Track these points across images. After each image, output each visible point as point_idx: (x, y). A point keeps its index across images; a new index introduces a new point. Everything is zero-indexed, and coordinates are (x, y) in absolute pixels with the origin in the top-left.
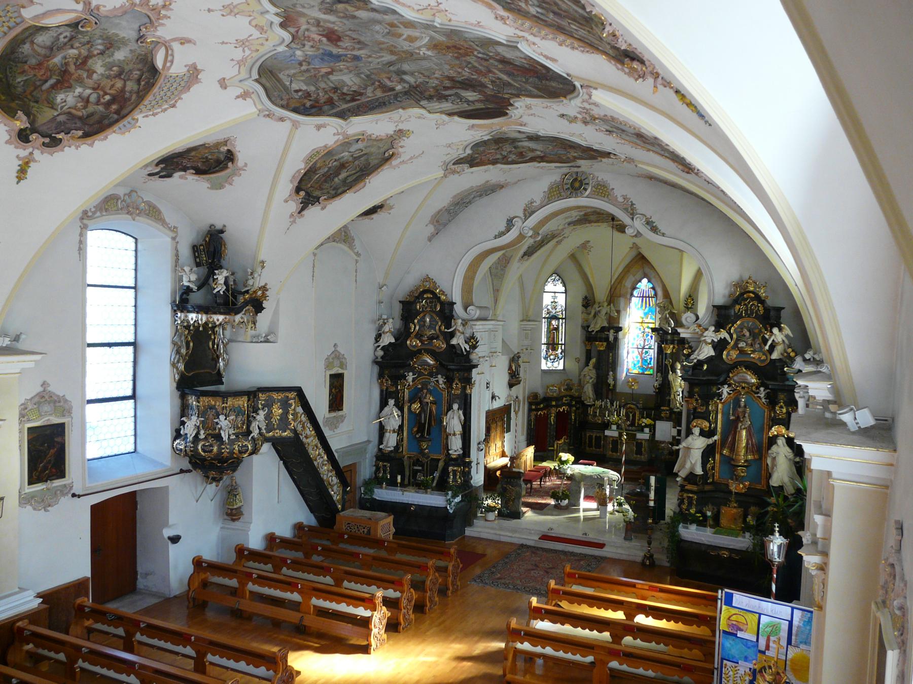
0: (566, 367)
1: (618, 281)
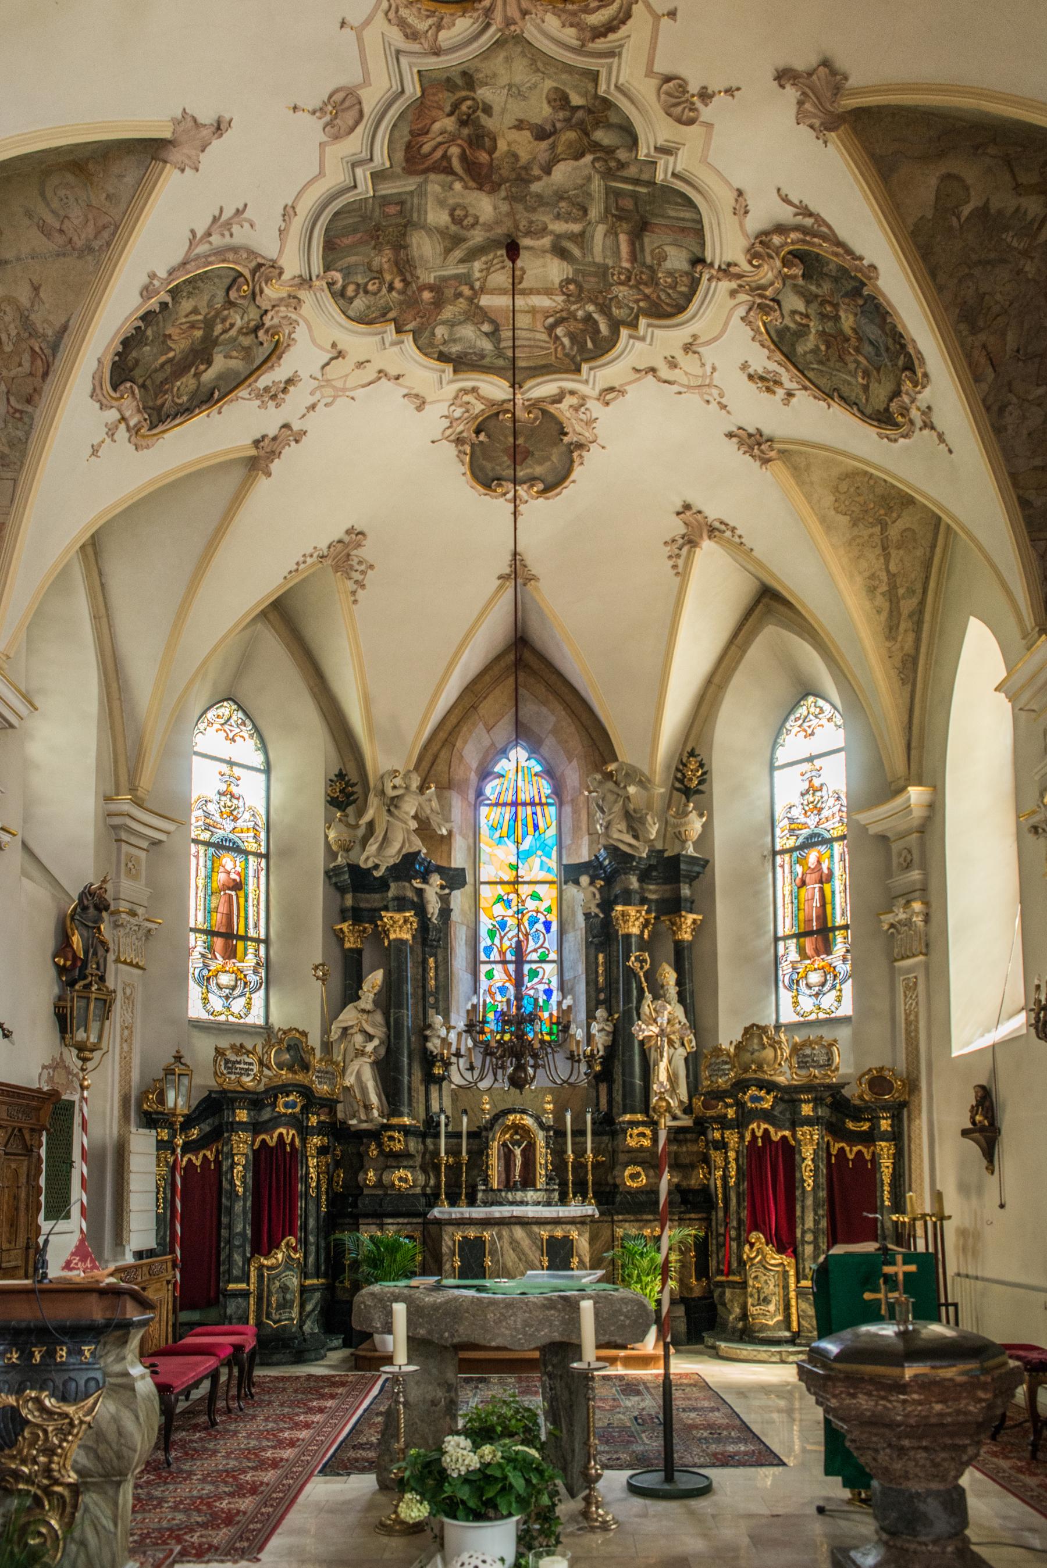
0: (276, 1020)
1: (442, 735)
